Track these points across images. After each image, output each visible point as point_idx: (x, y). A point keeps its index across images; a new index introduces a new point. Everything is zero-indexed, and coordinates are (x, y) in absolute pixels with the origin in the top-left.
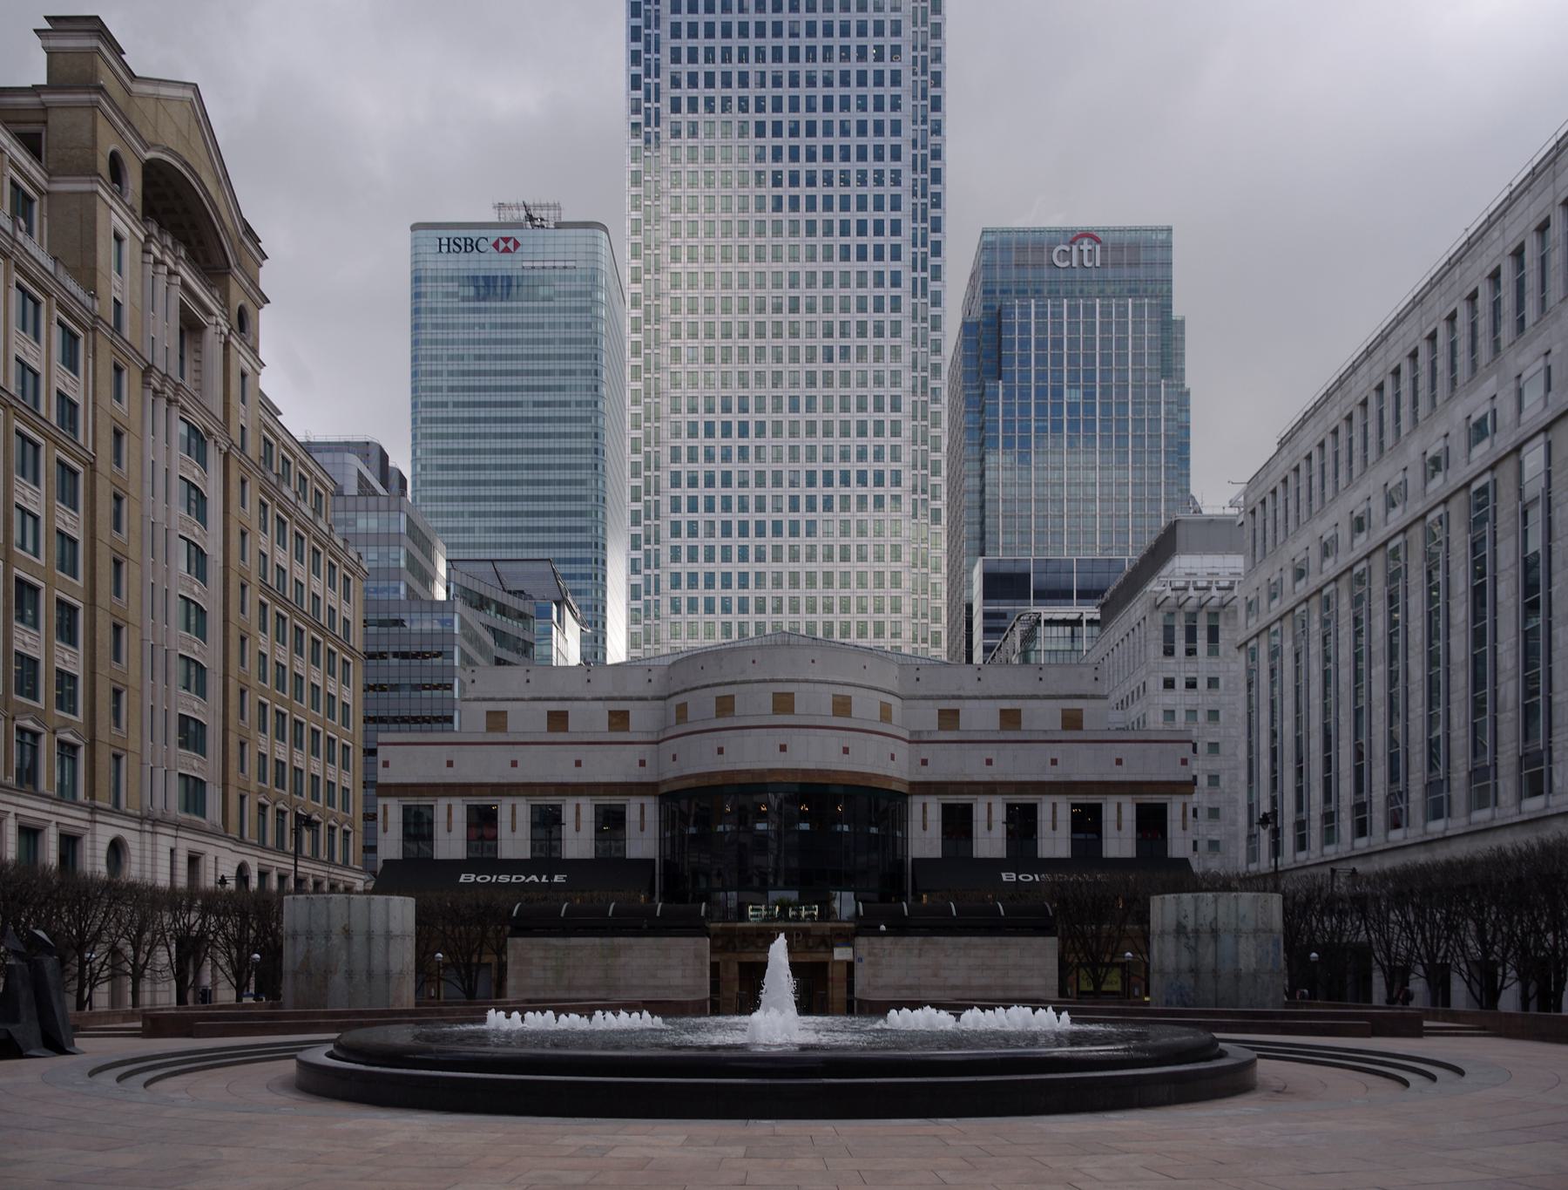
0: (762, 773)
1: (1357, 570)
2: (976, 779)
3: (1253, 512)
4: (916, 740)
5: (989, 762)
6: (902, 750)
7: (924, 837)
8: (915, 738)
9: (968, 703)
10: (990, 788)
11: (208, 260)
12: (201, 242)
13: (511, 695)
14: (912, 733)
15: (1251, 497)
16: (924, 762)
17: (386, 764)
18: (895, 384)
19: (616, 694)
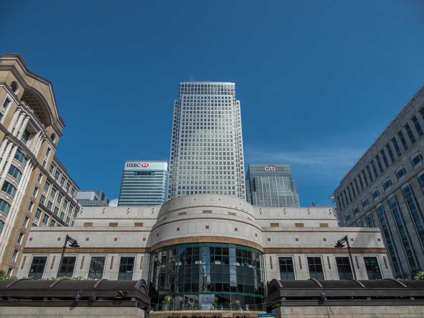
0: (197, 238)
1: (377, 207)
2: (292, 247)
3: (338, 198)
4: (264, 231)
5: (297, 240)
6: (260, 234)
7: (270, 271)
8: (264, 230)
9: (282, 221)
10: (300, 250)
11: (46, 122)
12: (44, 118)
13: (96, 217)
14: (263, 228)
15: (337, 194)
16: (269, 240)
17: (31, 239)
18: (234, 184)
19: (138, 217)
